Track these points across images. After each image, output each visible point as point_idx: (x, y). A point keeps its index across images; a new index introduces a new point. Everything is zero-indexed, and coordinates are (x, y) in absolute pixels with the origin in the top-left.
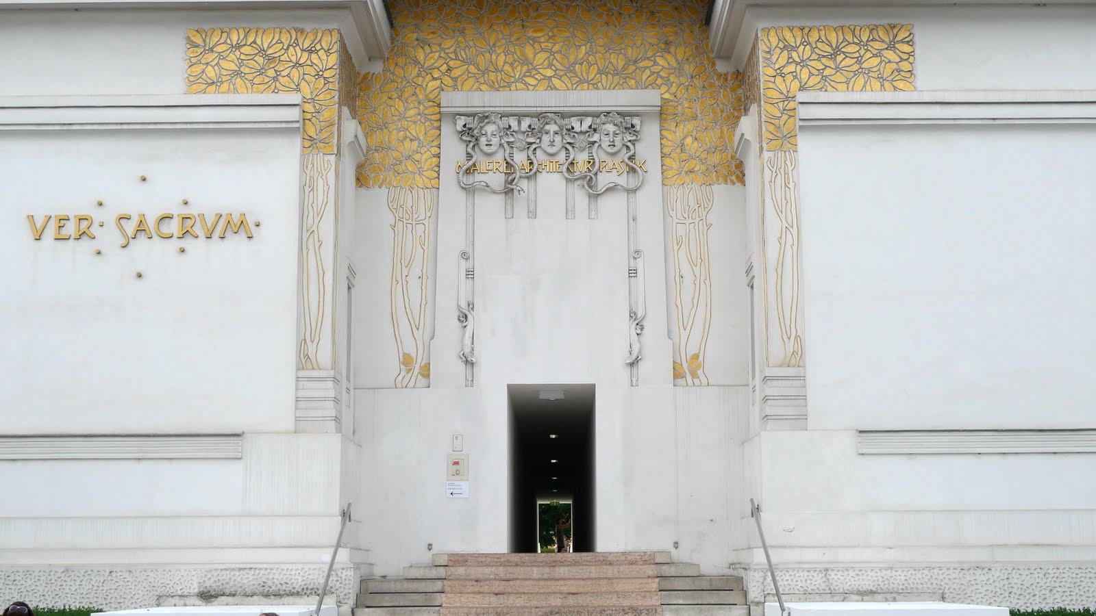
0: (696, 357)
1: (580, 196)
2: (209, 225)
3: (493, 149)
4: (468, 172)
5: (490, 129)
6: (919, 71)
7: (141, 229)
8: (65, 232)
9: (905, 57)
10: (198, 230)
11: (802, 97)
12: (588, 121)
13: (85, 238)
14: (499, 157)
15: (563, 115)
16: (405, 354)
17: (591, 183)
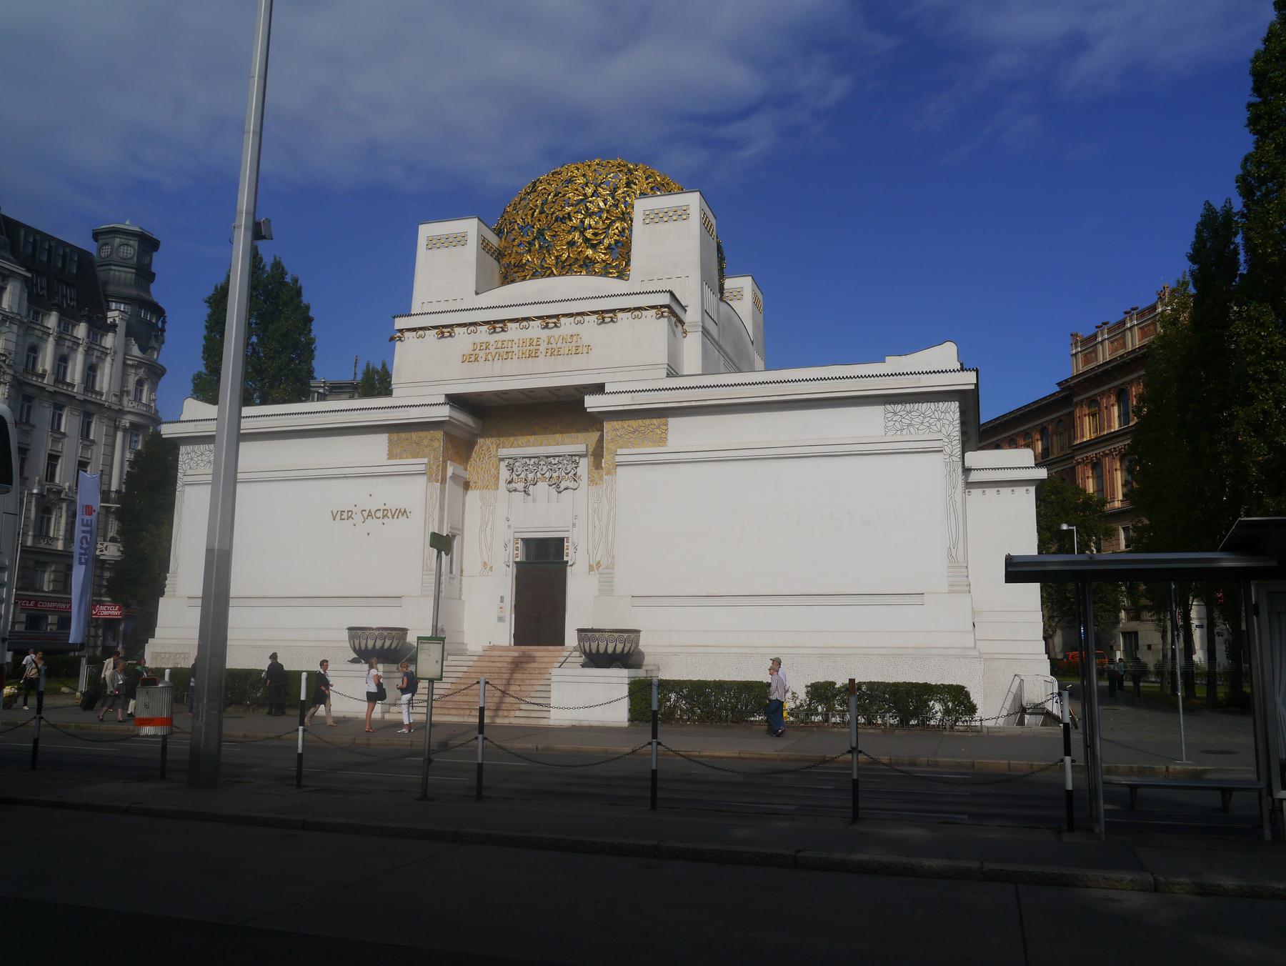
0: (599, 562)
1: (553, 491)
2: (393, 513)
3: (519, 473)
4: (510, 482)
5: (517, 464)
6: (670, 436)
7: (370, 515)
8: (343, 517)
9: (664, 431)
10: (389, 515)
11: (619, 451)
12: (557, 459)
13: (350, 519)
14: (523, 476)
15: (547, 457)
16: (485, 563)
17: (558, 487)
